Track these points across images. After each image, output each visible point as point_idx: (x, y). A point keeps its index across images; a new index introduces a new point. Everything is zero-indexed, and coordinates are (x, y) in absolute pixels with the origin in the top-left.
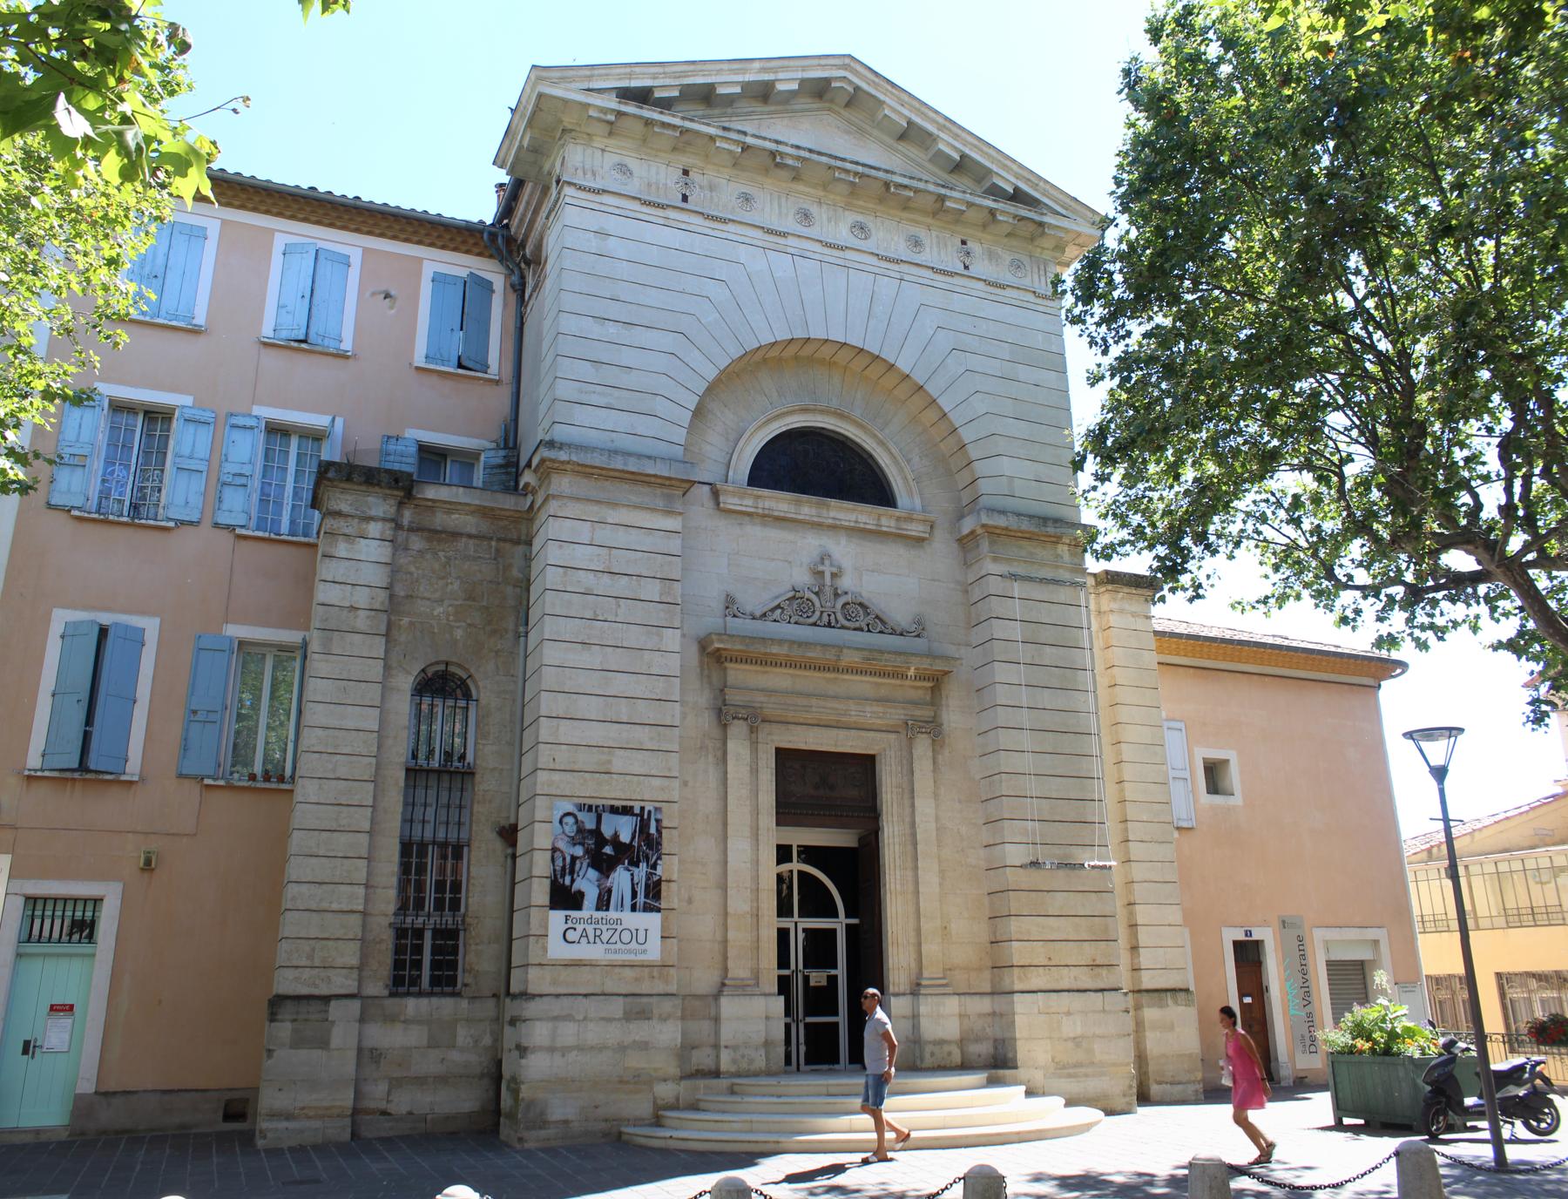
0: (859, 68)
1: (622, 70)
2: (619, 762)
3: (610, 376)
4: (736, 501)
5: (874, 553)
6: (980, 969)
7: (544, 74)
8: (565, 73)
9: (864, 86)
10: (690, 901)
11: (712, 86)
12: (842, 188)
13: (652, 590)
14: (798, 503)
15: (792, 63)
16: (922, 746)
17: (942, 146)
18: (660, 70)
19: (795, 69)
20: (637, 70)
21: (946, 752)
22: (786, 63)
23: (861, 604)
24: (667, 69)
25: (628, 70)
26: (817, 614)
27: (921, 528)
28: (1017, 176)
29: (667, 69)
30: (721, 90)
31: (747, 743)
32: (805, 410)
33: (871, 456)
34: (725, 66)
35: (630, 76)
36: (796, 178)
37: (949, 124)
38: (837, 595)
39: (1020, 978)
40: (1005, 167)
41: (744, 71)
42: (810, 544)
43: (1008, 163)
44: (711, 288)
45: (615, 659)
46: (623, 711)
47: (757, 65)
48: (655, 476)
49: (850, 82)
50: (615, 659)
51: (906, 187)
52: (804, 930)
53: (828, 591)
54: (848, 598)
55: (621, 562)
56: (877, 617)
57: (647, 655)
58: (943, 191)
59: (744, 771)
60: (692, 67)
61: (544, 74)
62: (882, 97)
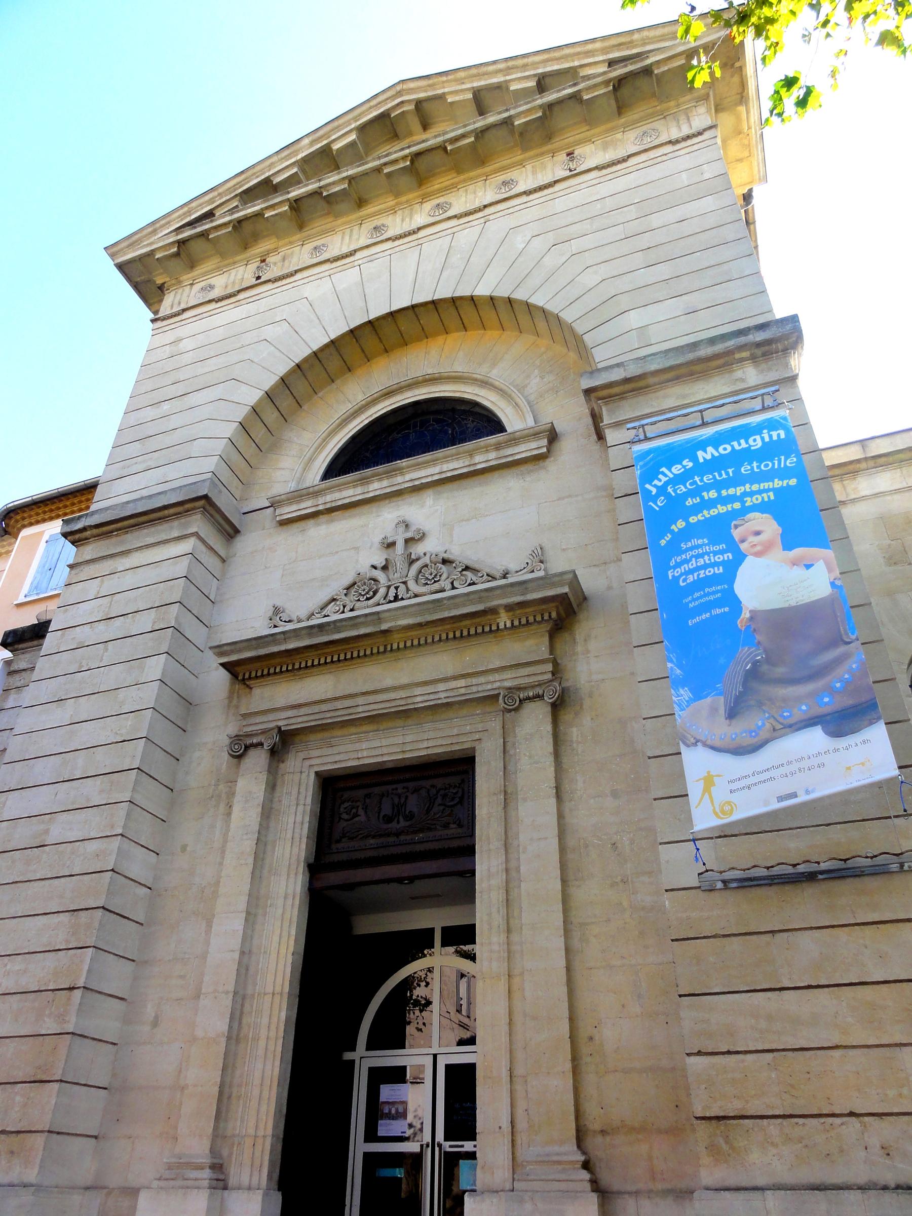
0: (412, 85)
1: (181, 212)
2: (58, 831)
3: (153, 444)
4: (294, 507)
5: (466, 498)
6: (675, 1131)
7: (115, 249)
8: (132, 240)
9: (422, 95)
10: (155, 1023)
11: (267, 181)
12: (405, 181)
13: (146, 622)
14: (364, 481)
15: (341, 121)
16: (535, 721)
17: (513, 87)
18: (215, 193)
19: (349, 123)
20: (194, 205)
21: (586, 720)
22: (336, 124)
23: (445, 562)
24: (220, 190)
25: (186, 209)
26: (382, 591)
27: (533, 445)
28: (604, 51)
29: (220, 190)
30: (277, 180)
31: (263, 777)
32: (389, 393)
33: (476, 404)
34: (275, 159)
35: (189, 213)
36: (361, 203)
37: (511, 63)
38: (412, 562)
39: (712, 1149)
40: (588, 54)
41: (296, 153)
42: (384, 521)
43: (590, 47)
44: (270, 332)
45: (86, 708)
46: (80, 764)
47: (306, 141)
48: (165, 507)
49: (409, 101)
50: (86, 708)
51: (463, 136)
52: (448, 1067)
53: (399, 563)
54: (426, 560)
55: (120, 605)
56: (467, 568)
57: (122, 694)
58: (506, 115)
59: (253, 816)
60: (243, 177)
61: (115, 249)
62: (440, 92)
